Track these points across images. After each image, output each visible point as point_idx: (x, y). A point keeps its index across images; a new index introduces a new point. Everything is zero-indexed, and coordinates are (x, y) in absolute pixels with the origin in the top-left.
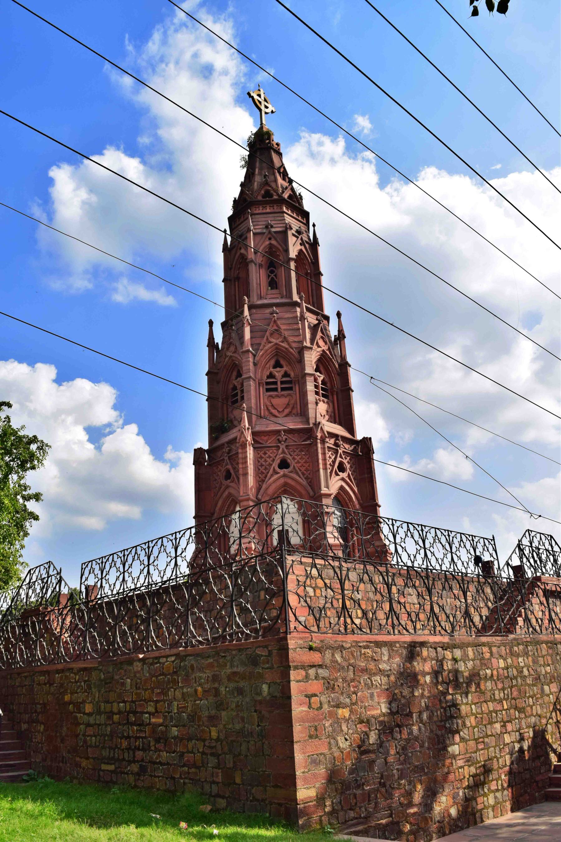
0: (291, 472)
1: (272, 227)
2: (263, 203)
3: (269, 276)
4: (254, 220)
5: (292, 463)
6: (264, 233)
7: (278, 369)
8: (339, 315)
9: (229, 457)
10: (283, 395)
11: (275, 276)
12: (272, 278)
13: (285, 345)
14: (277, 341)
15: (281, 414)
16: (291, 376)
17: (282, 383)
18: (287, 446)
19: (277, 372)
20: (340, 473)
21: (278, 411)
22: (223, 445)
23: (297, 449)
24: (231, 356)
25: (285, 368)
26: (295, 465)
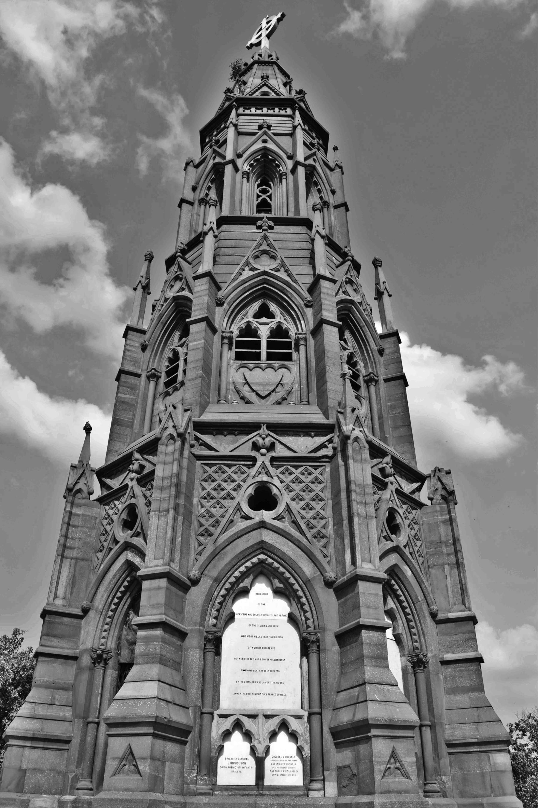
0: (279, 518)
1: (269, 127)
2: (259, 103)
3: (258, 196)
4: (239, 121)
5: (285, 499)
6: (254, 134)
7: (264, 320)
8: (376, 263)
9: (139, 481)
10: (270, 366)
11: (270, 197)
12: (264, 200)
13: (282, 275)
14: (267, 269)
15: (263, 401)
16: (290, 333)
17: (270, 345)
18: (273, 460)
19: (261, 323)
20: (393, 537)
21: (257, 394)
22: (131, 454)
23: (296, 467)
24: (175, 298)
25: (277, 319)
26: (293, 505)
